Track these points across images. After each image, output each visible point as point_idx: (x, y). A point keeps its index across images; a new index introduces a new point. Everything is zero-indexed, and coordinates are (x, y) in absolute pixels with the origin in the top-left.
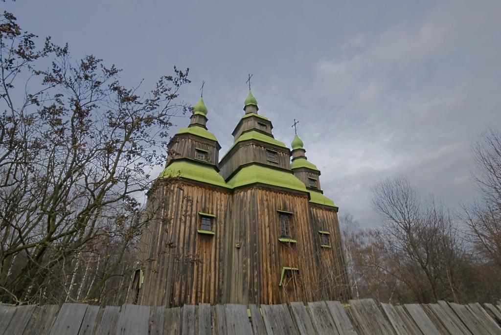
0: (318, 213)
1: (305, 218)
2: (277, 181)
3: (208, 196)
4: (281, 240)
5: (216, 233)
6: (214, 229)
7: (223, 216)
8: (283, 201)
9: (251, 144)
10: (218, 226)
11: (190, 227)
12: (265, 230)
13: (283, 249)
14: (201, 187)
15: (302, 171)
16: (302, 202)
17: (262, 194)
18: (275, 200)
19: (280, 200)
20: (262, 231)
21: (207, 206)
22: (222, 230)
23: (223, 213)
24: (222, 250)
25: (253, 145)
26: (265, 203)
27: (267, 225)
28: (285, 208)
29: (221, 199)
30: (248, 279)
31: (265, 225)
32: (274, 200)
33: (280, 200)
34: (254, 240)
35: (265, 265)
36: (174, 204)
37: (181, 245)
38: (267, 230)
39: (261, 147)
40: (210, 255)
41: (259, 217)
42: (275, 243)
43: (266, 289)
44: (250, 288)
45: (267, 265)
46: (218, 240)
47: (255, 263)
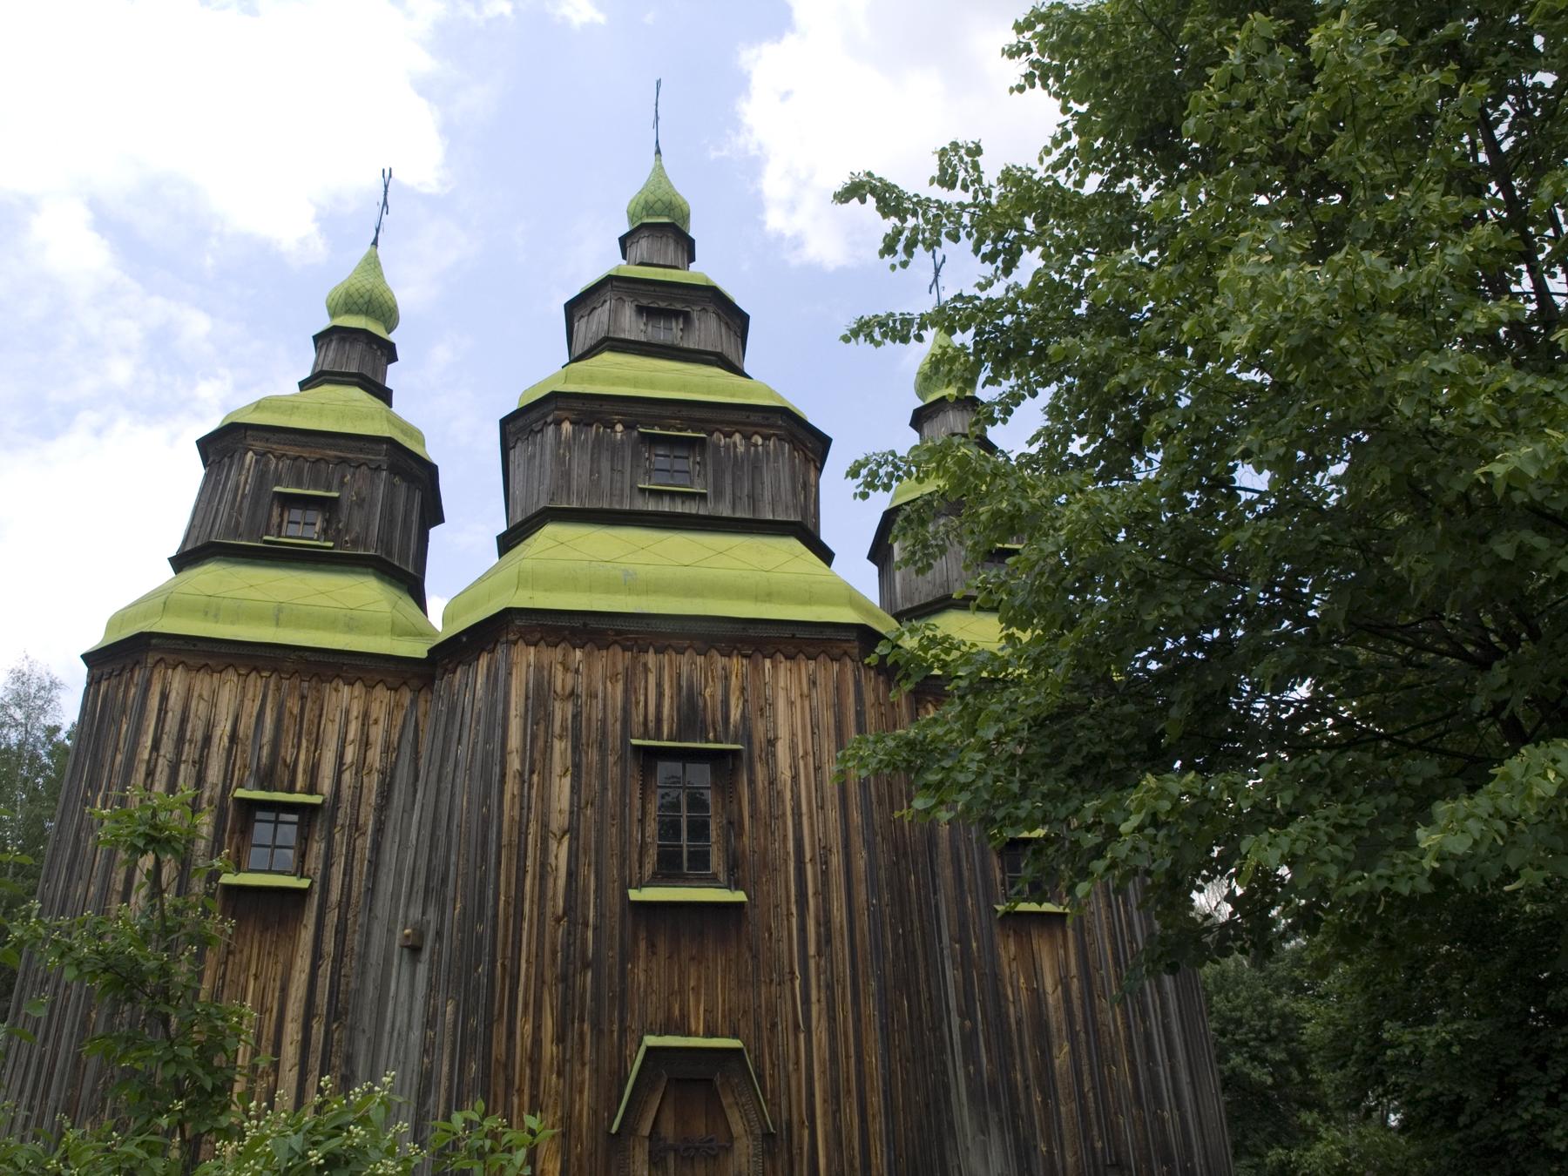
3: (293, 705)
6: (314, 862)
7: (371, 798)
10: (340, 849)
12: (545, 850)
13: (652, 946)
14: (255, 669)
16: (813, 683)
18: (626, 691)
19: (659, 685)
20: (522, 857)
21: (288, 753)
22: (361, 868)
24: (350, 965)
25: (558, 423)
26: (561, 712)
27: (558, 821)
28: (691, 717)
29: (366, 715)
31: (545, 826)
32: (620, 686)
33: (659, 685)
35: (524, 1028)
36: (119, 758)
40: (284, 990)
41: (511, 787)
42: (600, 915)
45: (537, 1028)
46: (332, 918)
47: (473, 1022)
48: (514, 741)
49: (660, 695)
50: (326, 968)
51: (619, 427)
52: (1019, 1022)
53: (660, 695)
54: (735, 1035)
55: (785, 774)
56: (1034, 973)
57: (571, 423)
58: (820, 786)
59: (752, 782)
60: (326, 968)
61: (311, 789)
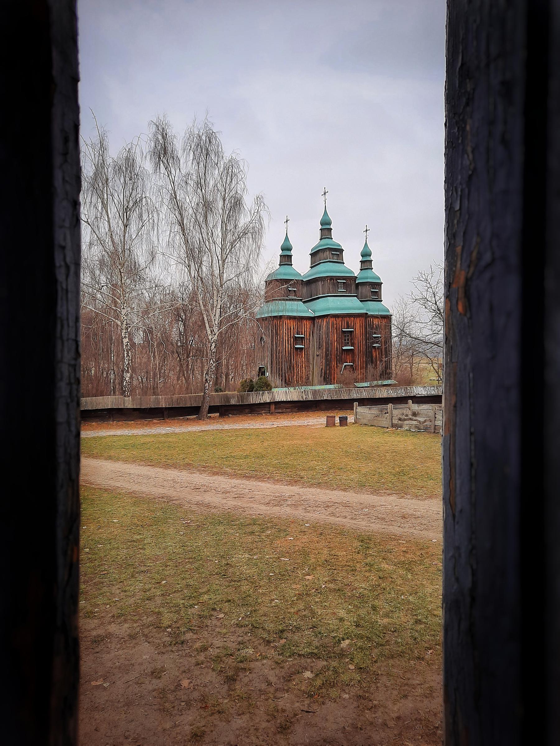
2: (343, 309)
4: (344, 348)
5: (305, 346)
7: (308, 335)
8: (347, 322)
9: (326, 279)
10: (306, 342)
11: (291, 344)
15: (366, 285)
16: (360, 320)
21: (299, 329)
23: (308, 333)
26: (335, 326)
30: (323, 371)
31: (334, 341)
34: (327, 350)
37: (287, 355)
43: (333, 376)
44: (325, 375)
50: (306, 356)
55: (357, 332)
60: (306, 356)
61: (302, 334)
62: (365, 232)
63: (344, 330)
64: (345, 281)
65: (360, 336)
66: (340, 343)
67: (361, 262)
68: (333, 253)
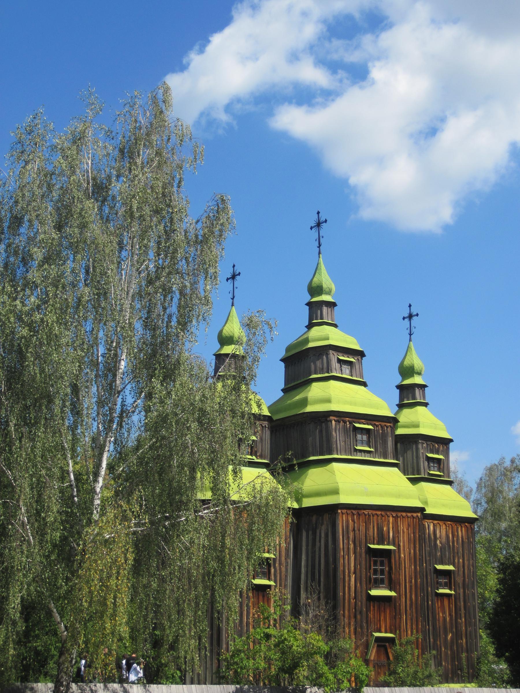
0: (438, 532)
1: (412, 551)
4: (374, 592)
10: (278, 571)
13: (374, 607)
17: (347, 521)
19: (373, 527)
31: (349, 572)
33: (373, 527)
38: (353, 579)
39: (345, 422)
41: (342, 561)
48: (342, 547)
49: (374, 530)
51: (348, 423)
52: (439, 627)
53: (374, 530)
54: (391, 633)
55: (402, 556)
56: (444, 612)
57: (335, 421)
58: (410, 560)
59: (395, 558)
62: (407, 320)
63: (372, 546)
64: (370, 427)
65: (410, 566)
66: (364, 580)
67: (398, 387)
68: (341, 358)
